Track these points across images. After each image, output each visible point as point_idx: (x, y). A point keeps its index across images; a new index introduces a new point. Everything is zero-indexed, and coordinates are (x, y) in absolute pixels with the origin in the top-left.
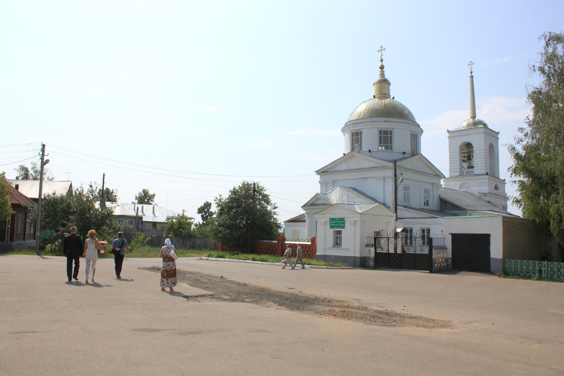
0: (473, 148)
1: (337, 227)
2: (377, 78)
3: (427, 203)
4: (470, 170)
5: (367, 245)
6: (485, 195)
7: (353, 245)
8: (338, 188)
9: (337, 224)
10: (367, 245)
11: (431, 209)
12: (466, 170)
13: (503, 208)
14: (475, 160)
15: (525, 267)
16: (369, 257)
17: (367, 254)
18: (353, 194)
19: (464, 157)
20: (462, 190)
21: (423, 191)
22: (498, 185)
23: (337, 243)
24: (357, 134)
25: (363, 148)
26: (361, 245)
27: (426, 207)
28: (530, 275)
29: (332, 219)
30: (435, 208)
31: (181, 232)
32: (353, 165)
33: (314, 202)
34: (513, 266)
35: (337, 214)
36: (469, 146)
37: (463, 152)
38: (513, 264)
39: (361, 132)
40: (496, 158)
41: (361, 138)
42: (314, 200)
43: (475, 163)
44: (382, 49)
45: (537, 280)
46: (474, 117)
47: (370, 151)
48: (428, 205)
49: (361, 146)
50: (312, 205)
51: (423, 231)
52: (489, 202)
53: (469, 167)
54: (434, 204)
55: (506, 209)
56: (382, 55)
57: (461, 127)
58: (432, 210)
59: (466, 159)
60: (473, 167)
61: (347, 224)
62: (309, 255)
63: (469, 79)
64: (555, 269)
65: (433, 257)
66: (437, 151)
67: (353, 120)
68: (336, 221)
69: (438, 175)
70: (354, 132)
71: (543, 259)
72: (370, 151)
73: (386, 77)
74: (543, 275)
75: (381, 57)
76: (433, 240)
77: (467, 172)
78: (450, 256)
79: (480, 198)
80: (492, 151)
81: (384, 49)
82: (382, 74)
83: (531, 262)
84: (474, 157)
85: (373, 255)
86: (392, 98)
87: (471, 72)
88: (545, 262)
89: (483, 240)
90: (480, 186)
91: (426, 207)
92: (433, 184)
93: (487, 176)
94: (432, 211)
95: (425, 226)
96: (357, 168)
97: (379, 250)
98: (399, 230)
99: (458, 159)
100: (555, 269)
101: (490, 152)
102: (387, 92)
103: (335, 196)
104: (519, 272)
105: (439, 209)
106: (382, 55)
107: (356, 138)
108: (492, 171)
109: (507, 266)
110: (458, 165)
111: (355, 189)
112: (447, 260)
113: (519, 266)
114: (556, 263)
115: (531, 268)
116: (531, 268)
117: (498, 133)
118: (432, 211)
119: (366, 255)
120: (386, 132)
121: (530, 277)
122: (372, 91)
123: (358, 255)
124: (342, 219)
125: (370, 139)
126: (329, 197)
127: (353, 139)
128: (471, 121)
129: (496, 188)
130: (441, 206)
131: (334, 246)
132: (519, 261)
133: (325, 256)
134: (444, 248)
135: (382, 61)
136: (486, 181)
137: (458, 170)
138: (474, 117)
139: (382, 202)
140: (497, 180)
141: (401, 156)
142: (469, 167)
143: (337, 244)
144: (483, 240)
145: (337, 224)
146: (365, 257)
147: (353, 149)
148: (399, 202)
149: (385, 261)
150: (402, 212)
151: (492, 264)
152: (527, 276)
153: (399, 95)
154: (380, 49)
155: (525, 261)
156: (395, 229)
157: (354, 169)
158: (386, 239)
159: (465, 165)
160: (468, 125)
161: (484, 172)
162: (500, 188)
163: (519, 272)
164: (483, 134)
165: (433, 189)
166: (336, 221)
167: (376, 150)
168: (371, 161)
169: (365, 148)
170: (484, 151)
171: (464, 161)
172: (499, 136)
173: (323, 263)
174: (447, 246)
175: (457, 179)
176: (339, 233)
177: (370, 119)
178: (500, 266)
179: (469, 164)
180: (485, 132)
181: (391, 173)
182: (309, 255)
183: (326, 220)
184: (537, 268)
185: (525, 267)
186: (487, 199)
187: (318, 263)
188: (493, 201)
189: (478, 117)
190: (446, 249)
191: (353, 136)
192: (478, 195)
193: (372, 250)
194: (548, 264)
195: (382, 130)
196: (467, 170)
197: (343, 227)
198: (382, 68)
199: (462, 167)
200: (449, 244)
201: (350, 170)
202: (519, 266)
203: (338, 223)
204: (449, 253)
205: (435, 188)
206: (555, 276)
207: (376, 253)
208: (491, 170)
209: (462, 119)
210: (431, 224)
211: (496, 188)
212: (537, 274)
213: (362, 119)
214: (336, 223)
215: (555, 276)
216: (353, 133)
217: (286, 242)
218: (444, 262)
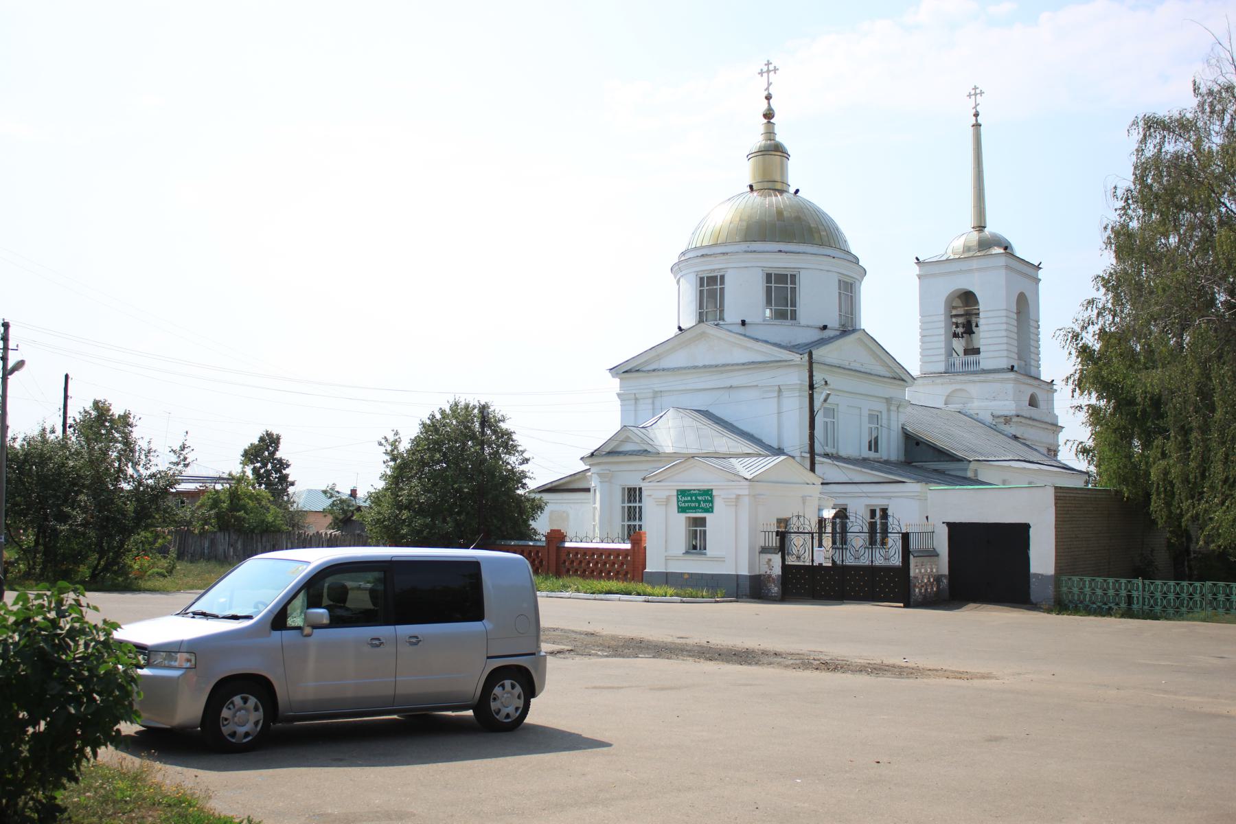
0: (976, 302)
1: (695, 509)
2: (757, 140)
3: (874, 445)
4: (971, 358)
5: (764, 550)
6: (1007, 420)
7: (732, 548)
8: (671, 412)
9: (695, 503)
10: (764, 550)
11: (885, 458)
12: (960, 359)
13: (1049, 450)
14: (982, 335)
15: (1099, 592)
16: (770, 576)
17: (763, 570)
18: (710, 429)
19: (957, 326)
20: (952, 407)
21: (865, 419)
22: (1038, 395)
23: (697, 542)
24: (712, 280)
25: (726, 316)
26: (751, 549)
27: (872, 455)
28: (1110, 608)
29: (682, 493)
30: (893, 458)
31: (238, 519)
32: (702, 354)
33: (618, 445)
34: (1076, 590)
35: (695, 479)
36: (968, 298)
37: (954, 312)
38: (1077, 585)
39: (722, 277)
40: (1032, 330)
41: (722, 290)
42: (615, 443)
43: (982, 342)
44: (769, 69)
45: (1122, 616)
46: (981, 228)
47: (743, 323)
48: (876, 451)
49: (722, 311)
50: (610, 453)
51: (873, 513)
52: (1015, 438)
53: (967, 352)
54: (891, 448)
55: (1056, 453)
56: (769, 84)
57: (950, 251)
58: (887, 462)
59: (960, 330)
60: (977, 351)
61: (718, 504)
62: (617, 573)
63: (970, 131)
64: (1158, 595)
65: (912, 574)
66: (896, 318)
67: (702, 247)
68: (691, 495)
69: (900, 377)
70: (705, 275)
71: (1137, 572)
72: (743, 323)
73: (780, 138)
74: (1135, 607)
75: (767, 89)
76: (911, 537)
77: (964, 364)
78: (945, 570)
79: (993, 428)
80: (1024, 310)
81: (775, 70)
82: (770, 132)
83: (1111, 580)
84: (981, 328)
85: (777, 570)
86: (792, 190)
87: (976, 115)
88: (1139, 581)
89: (1018, 534)
90: (994, 399)
91: (872, 455)
92: (888, 401)
93: (1012, 375)
94: (885, 465)
95: (878, 502)
96: (713, 363)
97: (791, 561)
98: (828, 514)
99: (942, 331)
100: (1158, 595)
101: (1018, 313)
102: (778, 178)
103: (668, 433)
104: (1087, 602)
105: (902, 458)
106: (769, 84)
107: (710, 293)
108: (1023, 366)
109: (1064, 589)
110: (943, 345)
111: (706, 414)
112: (938, 579)
113: (1087, 590)
114: (1159, 582)
115: (1111, 592)
116: (1111, 592)
117: (1038, 267)
118: (885, 465)
119: (762, 572)
120: (781, 278)
121: (1108, 613)
122: (745, 173)
123: (744, 571)
124: (708, 492)
125: (745, 294)
126: (651, 435)
127: (701, 292)
128: (974, 236)
129: (1033, 402)
130: (907, 451)
131: (687, 553)
132: (1087, 579)
133: (667, 574)
134: (933, 554)
135: (768, 98)
136: (1010, 387)
137: (943, 358)
138: (981, 228)
139: (775, 445)
140: (1035, 383)
141: (816, 335)
142: (967, 352)
143: (695, 547)
144: (1018, 534)
145: (695, 503)
146: (760, 576)
147: (701, 321)
148: (818, 448)
149: (804, 585)
150: (826, 469)
151: (1032, 586)
152: (1103, 610)
153: (809, 182)
154: (765, 69)
155: (1100, 580)
156: (820, 510)
157: (705, 367)
158: (808, 537)
159: (959, 345)
160: (967, 249)
161: (1004, 364)
162: (1042, 404)
163: (1087, 602)
164: (1003, 272)
165: (889, 410)
166: (691, 495)
167: (759, 320)
168: (747, 348)
169: (732, 314)
170: (1004, 313)
171: (955, 335)
172: (1041, 274)
173: (671, 591)
174: (938, 550)
175: (939, 381)
176: (701, 522)
177: (744, 246)
178: (1051, 590)
179: (967, 343)
180: (1007, 267)
181: (798, 377)
182: (626, 573)
183: (667, 493)
184: (1123, 593)
185: (1099, 592)
186: (1011, 430)
187: (662, 592)
188: (1026, 436)
189: (992, 228)
190: (937, 555)
191: (702, 285)
192: (989, 419)
193: (777, 559)
194: (1144, 584)
195: (773, 272)
196: (963, 358)
197: (710, 510)
198: (769, 115)
199: (950, 351)
200: (942, 544)
201: (695, 367)
202: (1087, 590)
203: (699, 502)
204: (943, 565)
205: (893, 408)
206: (1158, 609)
207: (785, 567)
208: (1020, 358)
209: (954, 236)
210: (890, 498)
211: (1033, 402)
212: (1123, 605)
213: (724, 244)
214: (691, 501)
215: (1158, 609)
216: (702, 279)
217: (567, 545)
218: (932, 584)
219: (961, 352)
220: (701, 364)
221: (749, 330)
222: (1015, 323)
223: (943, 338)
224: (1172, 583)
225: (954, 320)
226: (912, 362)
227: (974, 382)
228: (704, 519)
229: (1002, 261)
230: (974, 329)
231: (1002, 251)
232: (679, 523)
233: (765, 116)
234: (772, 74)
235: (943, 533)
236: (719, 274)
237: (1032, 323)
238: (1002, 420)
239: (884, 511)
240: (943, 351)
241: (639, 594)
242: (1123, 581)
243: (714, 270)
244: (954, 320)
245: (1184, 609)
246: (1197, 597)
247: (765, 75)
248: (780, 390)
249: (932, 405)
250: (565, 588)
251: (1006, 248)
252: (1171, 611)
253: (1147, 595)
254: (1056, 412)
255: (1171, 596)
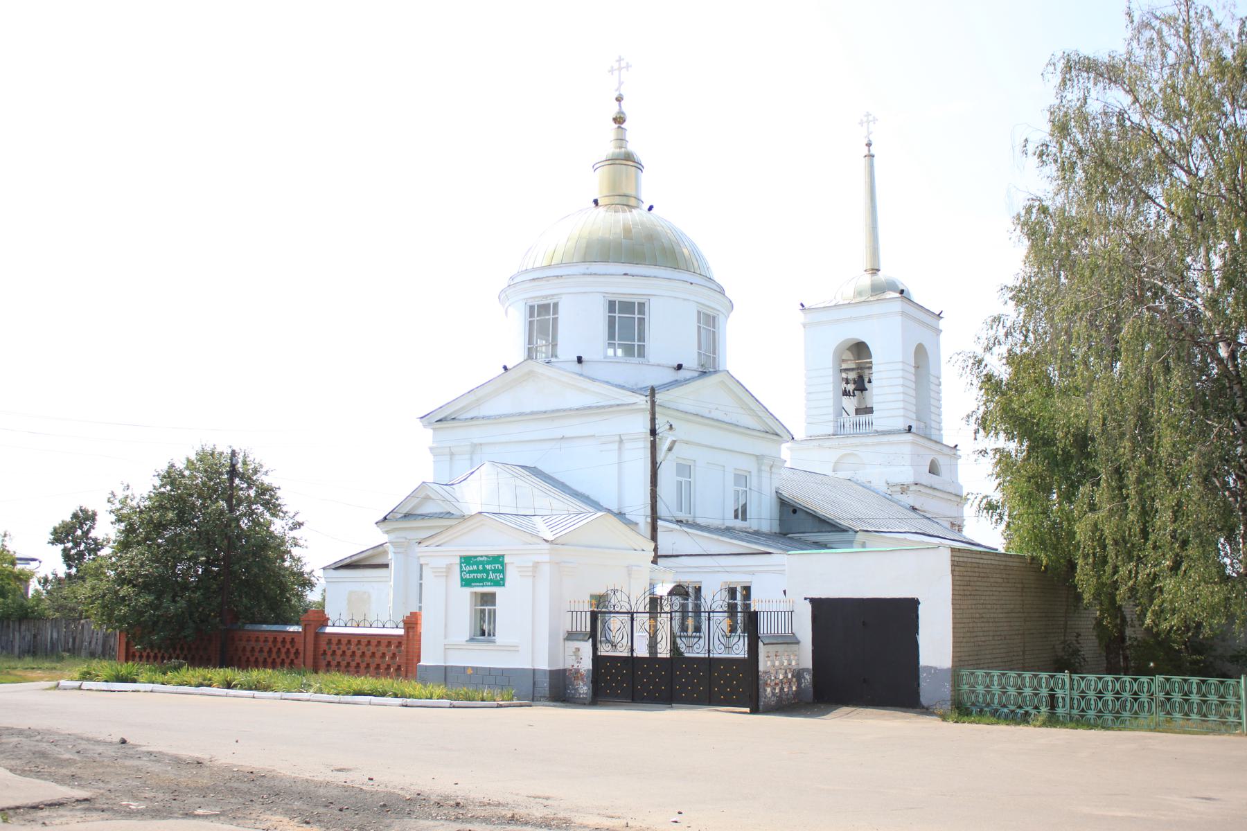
0: (870, 356)
3: (741, 513)
4: (863, 418)
5: (571, 636)
6: (904, 489)
8: (487, 468)
10: (571, 636)
11: (755, 527)
13: (953, 525)
14: (875, 391)
15: (1012, 691)
16: (577, 671)
17: (568, 663)
18: (531, 489)
20: (841, 475)
21: (730, 479)
23: (483, 630)
24: (544, 308)
25: (559, 352)
26: (552, 636)
27: (739, 524)
28: (1027, 712)
30: (765, 528)
32: (530, 398)
33: (413, 508)
34: (980, 689)
36: (860, 349)
37: (844, 366)
38: (982, 682)
39: (556, 305)
40: (933, 387)
41: (555, 320)
42: (414, 502)
43: (875, 399)
44: (621, 66)
47: (580, 360)
48: (744, 519)
49: (554, 346)
51: (732, 592)
52: (914, 509)
53: (858, 411)
54: (763, 515)
56: (621, 83)
58: (756, 533)
59: (851, 387)
60: (869, 411)
64: (1091, 695)
65: (761, 668)
67: (534, 269)
69: (775, 432)
70: (536, 303)
71: (1059, 665)
72: (580, 360)
73: (631, 147)
74: (1060, 711)
76: (761, 617)
77: (857, 425)
78: (808, 663)
79: (888, 498)
81: (628, 66)
82: (621, 140)
83: (1027, 675)
85: (586, 664)
88: (1066, 676)
89: (900, 616)
91: (739, 524)
93: (909, 437)
95: (738, 580)
96: (544, 409)
97: (605, 650)
98: (662, 590)
99: (830, 387)
100: (1091, 695)
101: (917, 367)
102: (631, 192)
103: (477, 492)
105: (776, 529)
106: (621, 83)
107: (542, 319)
108: (921, 427)
109: (965, 687)
110: (831, 403)
111: (535, 471)
112: (798, 674)
113: (996, 688)
114: (1092, 677)
115: (1028, 691)
116: (1028, 691)
119: (568, 666)
121: (1025, 719)
123: (543, 665)
125: (582, 326)
126: (458, 495)
127: (531, 323)
128: (866, 280)
129: (933, 469)
130: (782, 521)
131: (472, 640)
132: (996, 673)
133: (446, 667)
134: (791, 640)
136: (907, 449)
137: (831, 417)
138: (875, 271)
139: (615, 509)
140: (937, 447)
142: (858, 411)
143: (483, 634)
144: (900, 616)
146: (565, 671)
147: (531, 354)
149: (624, 682)
151: (923, 684)
153: (668, 201)
154: (616, 66)
155: (1012, 674)
156: (652, 586)
157: (532, 413)
158: (626, 618)
159: (850, 404)
161: (901, 424)
162: (943, 469)
164: (899, 319)
165: (760, 470)
167: (600, 357)
169: (567, 352)
170: (900, 366)
171: (846, 393)
172: (942, 324)
173: (439, 691)
174: (798, 636)
175: (827, 443)
176: (489, 599)
177: (582, 268)
178: (946, 690)
179: (859, 402)
182: (399, 668)
184: (1044, 692)
185: (1012, 691)
186: (909, 500)
187: (426, 692)
188: (925, 508)
190: (798, 643)
191: (531, 315)
192: (883, 488)
193: (586, 647)
194: (1071, 680)
198: (619, 120)
200: (804, 629)
201: (521, 414)
202: (996, 688)
204: (804, 656)
206: (1091, 713)
207: (597, 659)
208: (918, 419)
210: (753, 573)
211: (933, 469)
212: (1044, 709)
213: (559, 265)
215: (1091, 713)
216: (532, 308)
217: (328, 630)
218: (790, 682)
219: (852, 412)
220: (528, 410)
221: (584, 368)
222: (913, 378)
223: (831, 395)
224: (1109, 678)
225: (844, 375)
226: (795, 422)
227: (866, 445)
228: (493, 595)
229: (898, 306)
230: (867, 385)
231: (898, 295)
232: (463, 599)
233: (615, 120)
234: (624, 71)
236: (551, 302)
237: (932, 379)
238: (898, 489)
239: (747, 589)
240: (831, 410)
241: (396, 696)
242: (1044, 675)
243: (546, 297)
244: (844, 375)
245: (1126, 714)
246: (1144, 697)
247: (616, 73)
248: (621, 441)
249: (812, 464)
250: (305, 687)
251: (902, 292)
252: (1109, 717)
253: (1076, 694)
254: (961, 481)
255: (1109, 696)
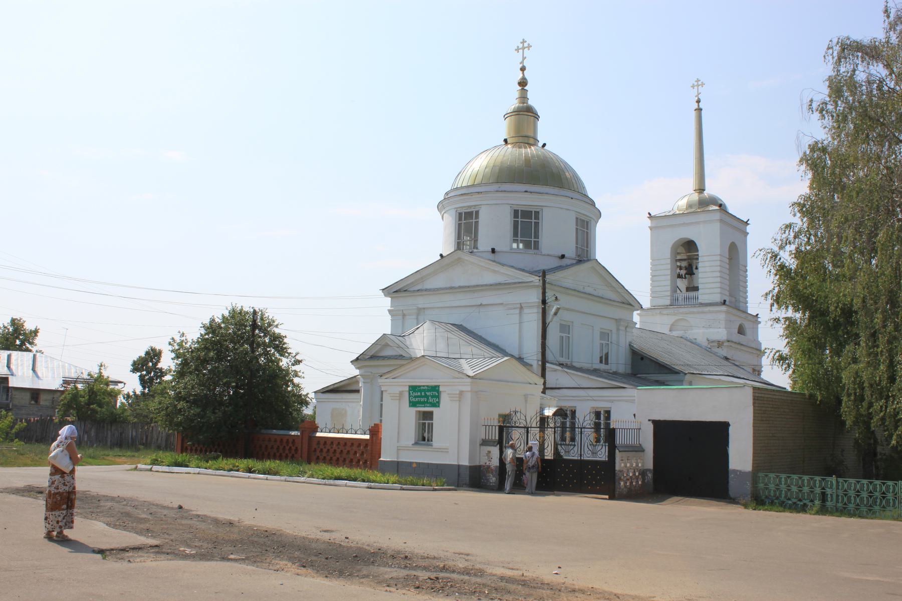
0: (697, 251)
1: (424, 404)
2: (513, 103)
3: (605, 359)
4: (692, 294)
5: (485, 443)
6: (720, 344)
7: (455, 440)
10: (485, 443)
12: (682, 294)
13: (754, 370)
14: (700, 275)
15: (794, 489)
16: (489, 467)
17: (483, 461)
18: (458, 340)
19: (681, 268)
20: (675, 333)
21: (597, 335)
22: (745, 326)
23: (424, 436)
24: (469, 215)
27: (603, 367)
28: (805, 505)
30: (621, 370)
34: (772, 487)
36: (690, 245)
37: (679, 257)
39: (477, 213)
40: (741, 273)
41: (477, 223)
43: (700, 281)
44: (524, 46)
46: (701, 190)
47: (493, 251)
48: (607, 363)
49: (476, 241)
50: (373, 357)
51: (598, 414)
52: (727, 359)
54: (620, 361)
55: (759, 373)
56: (524, 58)
57: (675, 208)
58: (615, 373)
59: (683, 272)
60: (696, 289)
62: (365, 462)
63: (693, 115)
64: (852, 493)
65: (617, 468)
66: (627, 254)
67: (462, 187)
69: (629, 302)
70: (463, 211)
71: (828, 471)
72: (493, 251)
73: (530, 102)
74: (829, 504)
75: (522, 62)
77: (687, 299)
78: (650, 465)
80: (734, 257)
82: (523, 97)
83: (806, 478)
84: (700, 269)
86: (540, 144)
87: (698, 101)
90: (710, 327)
91: (603, 367)
92: (618, 321)
93: (724, 308)
94: (614, 375)
95: (602, 405)
98: (549, 412)
99: (669, 272)
100: (852, 493)
101: (730, 259)
102: (531, 134)
103: (421, 341)
104: (783, 498)
105: (629, 371)
106: (524, 58)
107: (466, 224)
108: (734, 299)
109: (761, 486)
110: (669, 283)
112: (643, 473)
113: (783, 487)
114: (852, 481)
115: (806, 489)
116: (806, 489)
117: (746, 223)
118: (614, 375)
119: (482, 463)
121: (803, 509)
122: (503, 129)
123: (465, 462)
125: (495, 227)
126: (408, 343)
127: (460, 225)
128: (696, 197)
129: (741, 331)
131: (416, 443)
132: (783, 476)
133: (398, 463)
134: (639, 449)
135: (523, 69)
136: (722, 316)
137: (669, 293)
138: (701, 190)
139: (516, 354)
140: (744, 315)
143: (424, 439)
146: (480, 466)
147: (459, 246)
150: (556, 376)
153: (555, 139)
154: (521, 46)
155: (795, 477)
157: (460, 287)
158: (523, 431)
159: (682, 284)
160: (690, 206)
161: (718, 298)
162: (748, 332)
163: (783, 498)
164: (718, 225)
165: (618, 330)
167: (507, 249)
168: (495, 271)
169: (484, 244)
170: (718, 258)
171: (679, 276)
172: (749, 229)
173: (394, 478)
174: (644, 446)
175: (665, 312)
176: (428, 416)
177: (495, 187)
178: (748, 486)
179: (689, 283)
180: (721, 221)
182: (365, 462)
184: (818, 490)
185: (794, 489)
186: (723, 352)
187: (384, 479)
189: (711, 190)
190: (643, 451)
191: (460, 219)
192: (705, 343)
193: (495, 451)
194: (838, 482)
196: (685, 294)
197: (437, 405)
198: (523, 83)
199: (675, 289)
200: (648, 441)
201: (451, 288)
202: (783, 487)
204: (648, 461)
205: (622, 328)
206: (851, 506)
208: (731, 295)
209: (677, 195)
210: (612, 401)
211: (741, 331)
212: (817, 502)
213: (479, 185)
215: (851, 506)
216: (460, 214)
217: (318, 434)
218: (637, 478)
219: (684, 290)
220: (457, 285)
221: (497, 257)
222: (727, 266)
223: (669, 277)
224: (865, 482)
225: (678, 264)
227: (693, 313)
228: (431, 413)
229: (717, 216)
230: (695, 271)
231: (717, 208)
232: (410, 415)
233: (520, 84)
234: (526, 50)
235: (649, 429)
236: (474, 210)
237: (741, 268)
238: (716, 344)
239: (608, 413)
240: (669, 288)
241: (364, 481)
242: (818, 478)
243: (470, 207)
244: (678, 264)
245: (877, 508)
246: (890, 496)
247: (521, 51)
248: (521, 308)
250: (302, 473)
251: (720, 206)
252: (864, 509)
253: (841, 493)
254: (760, 339)
255: (864, 495)
